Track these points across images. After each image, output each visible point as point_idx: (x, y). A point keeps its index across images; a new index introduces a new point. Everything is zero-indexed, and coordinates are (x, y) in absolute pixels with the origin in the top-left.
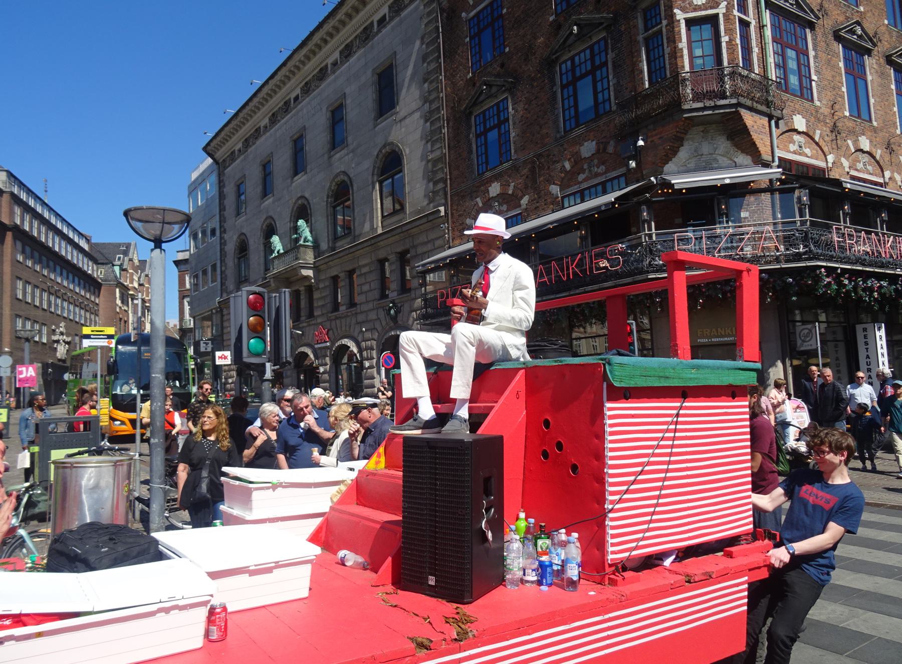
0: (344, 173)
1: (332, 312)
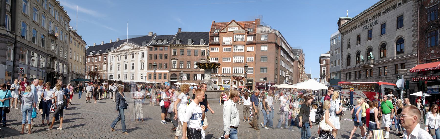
0: (385, 41)
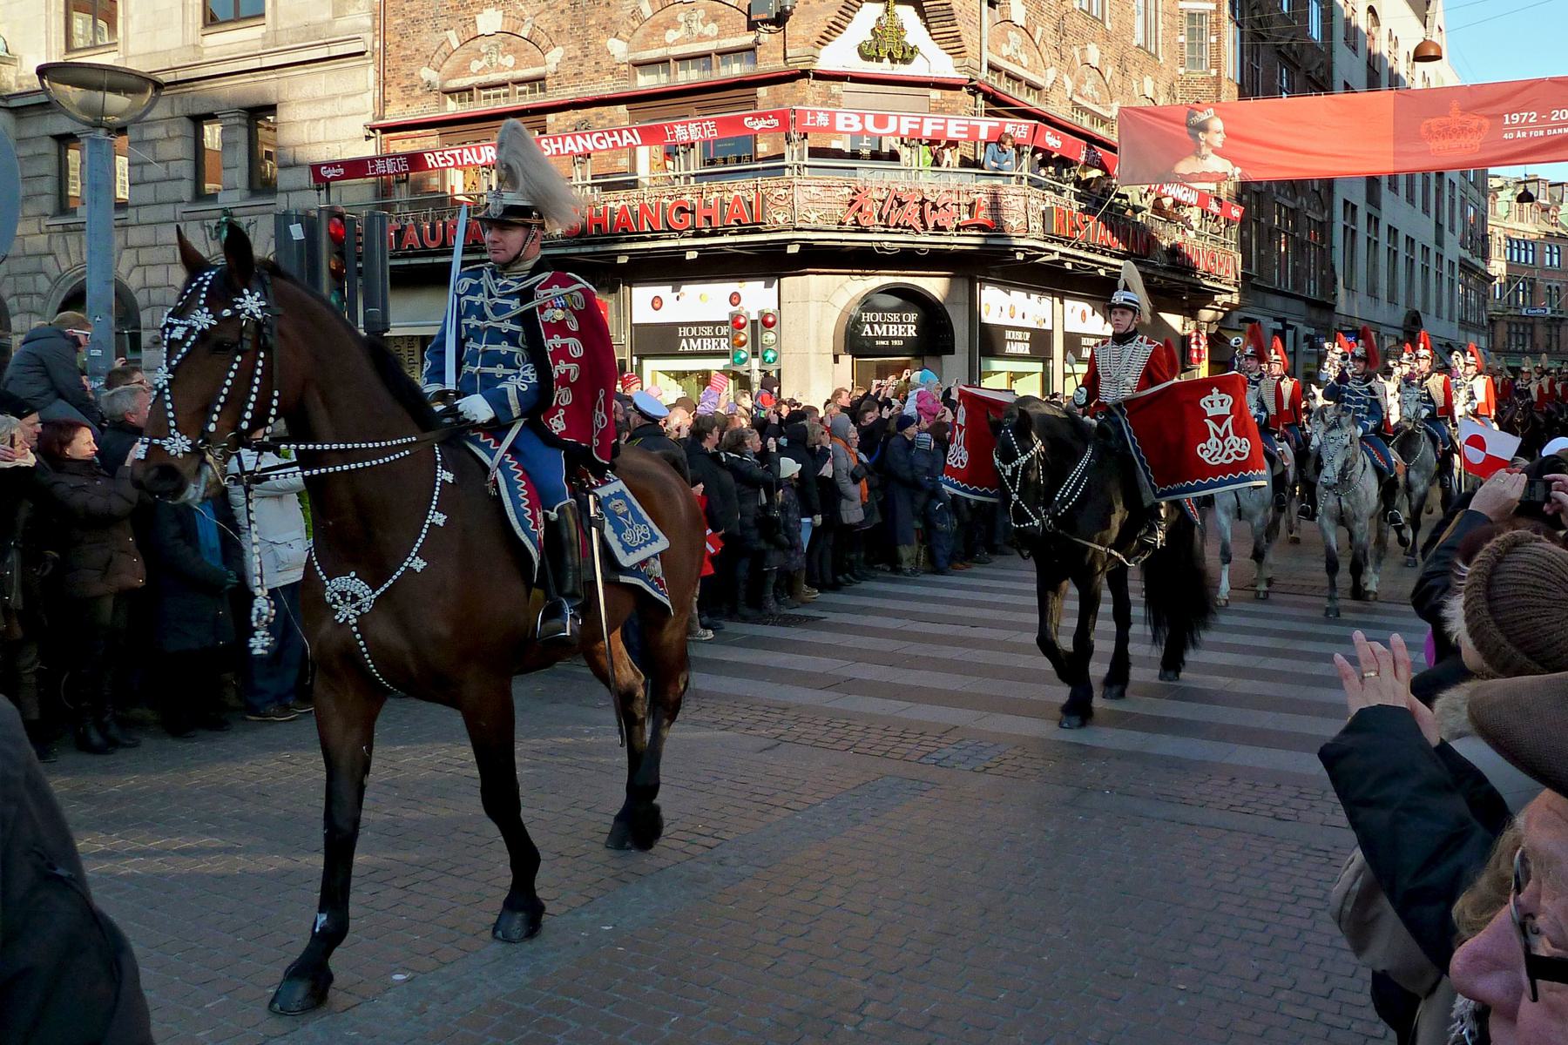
1: (53, 216)
